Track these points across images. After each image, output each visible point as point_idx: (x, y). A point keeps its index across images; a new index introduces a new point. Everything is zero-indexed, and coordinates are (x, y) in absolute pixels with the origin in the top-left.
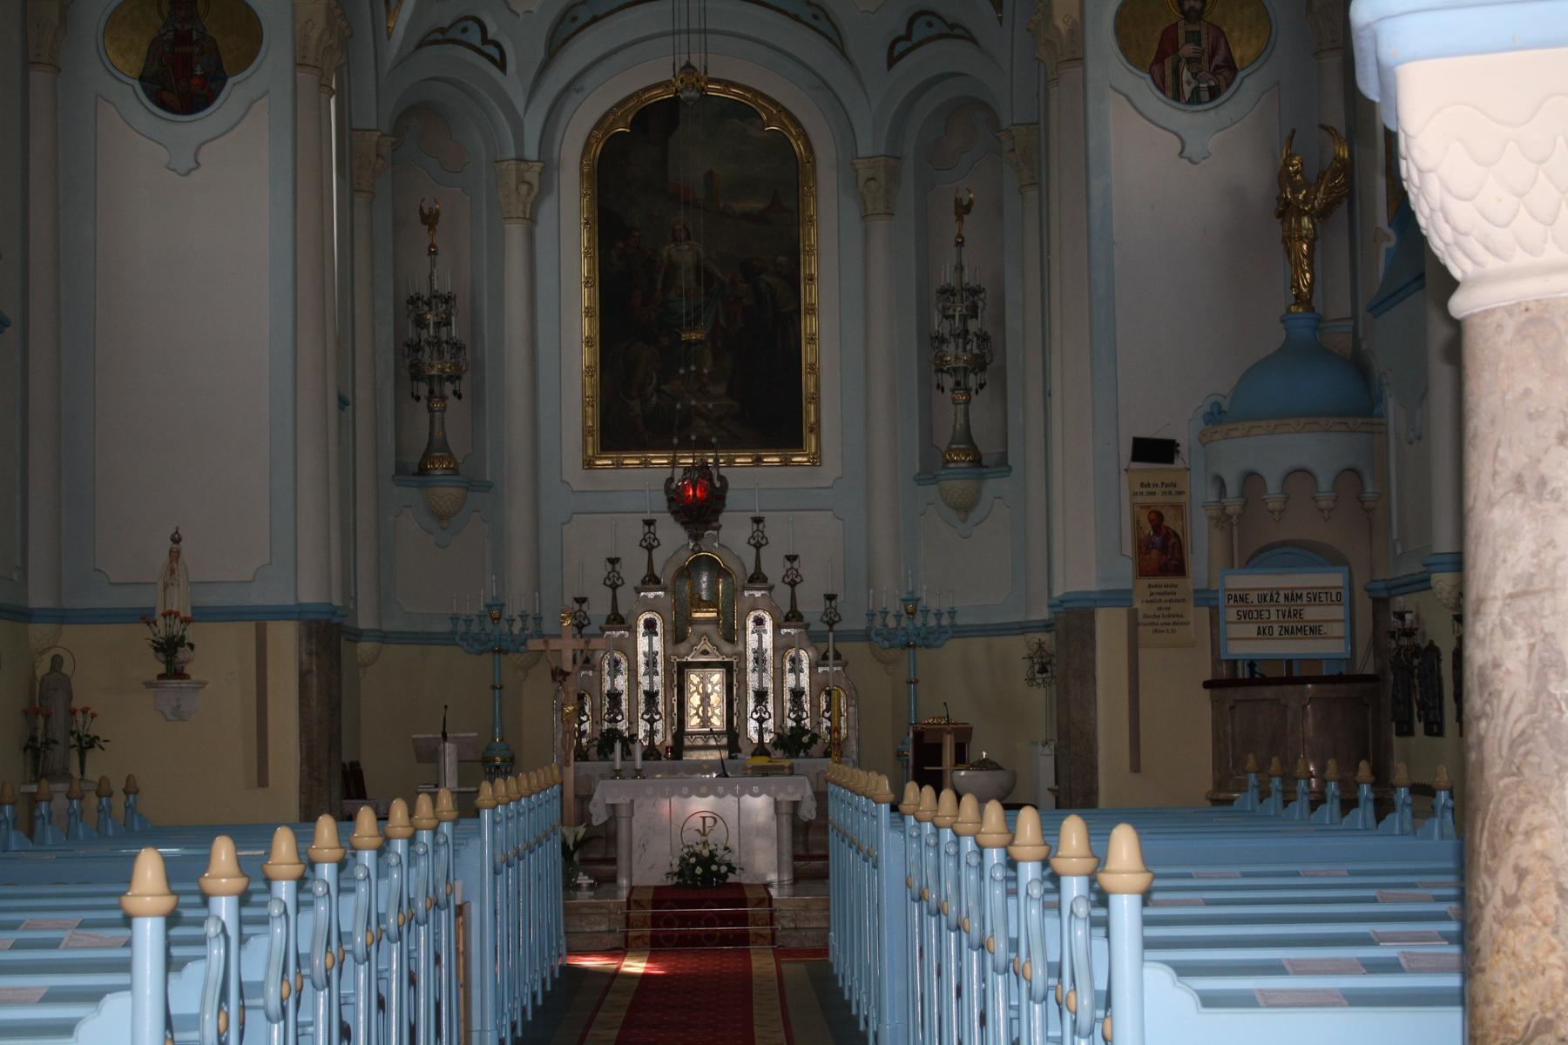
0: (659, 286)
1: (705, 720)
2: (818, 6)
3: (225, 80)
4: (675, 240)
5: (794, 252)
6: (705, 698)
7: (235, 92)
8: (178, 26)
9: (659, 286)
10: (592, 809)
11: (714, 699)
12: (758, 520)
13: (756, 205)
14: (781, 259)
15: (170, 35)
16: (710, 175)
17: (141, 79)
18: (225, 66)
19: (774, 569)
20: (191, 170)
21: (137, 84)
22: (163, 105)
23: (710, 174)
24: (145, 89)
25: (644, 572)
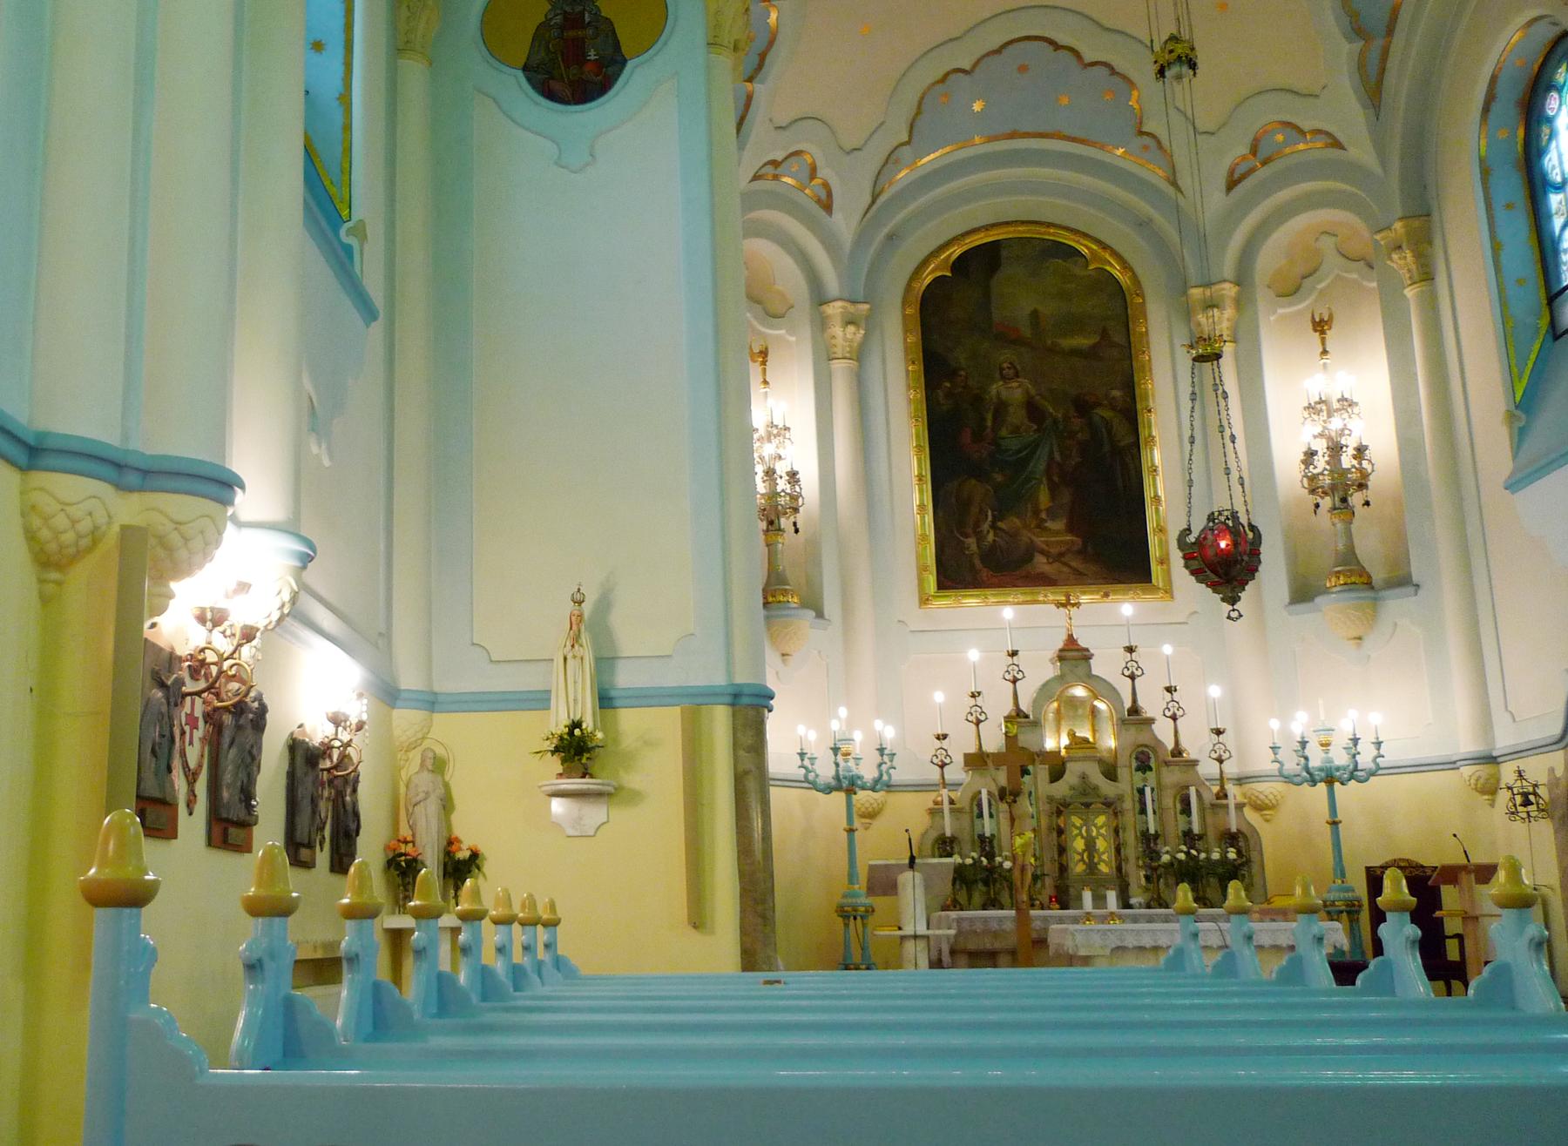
0: (989, 423)
1: (1092, 867)
2: (1148, 134)
3: (624, 62)
4: (1003, 377)
5: (1130, 387)
6: (1090, 846)
7: (635, 81)
8: (568, 9)
9: (989, 423)
10: (1414, 931)
11: (1101, 844)
12: (1130, 650)
13: (1083, 342)
14: (1116, 393)
15: (558, 19)
16: (1035, 314)
17: (525, 69)
18: (624, 49)
19: (1153, 704)
20: (587, 164)
21: (520, 74)
22: (550, 95)
23: (1035, 314)
24: (529, 80)
25: (1008, 708)
